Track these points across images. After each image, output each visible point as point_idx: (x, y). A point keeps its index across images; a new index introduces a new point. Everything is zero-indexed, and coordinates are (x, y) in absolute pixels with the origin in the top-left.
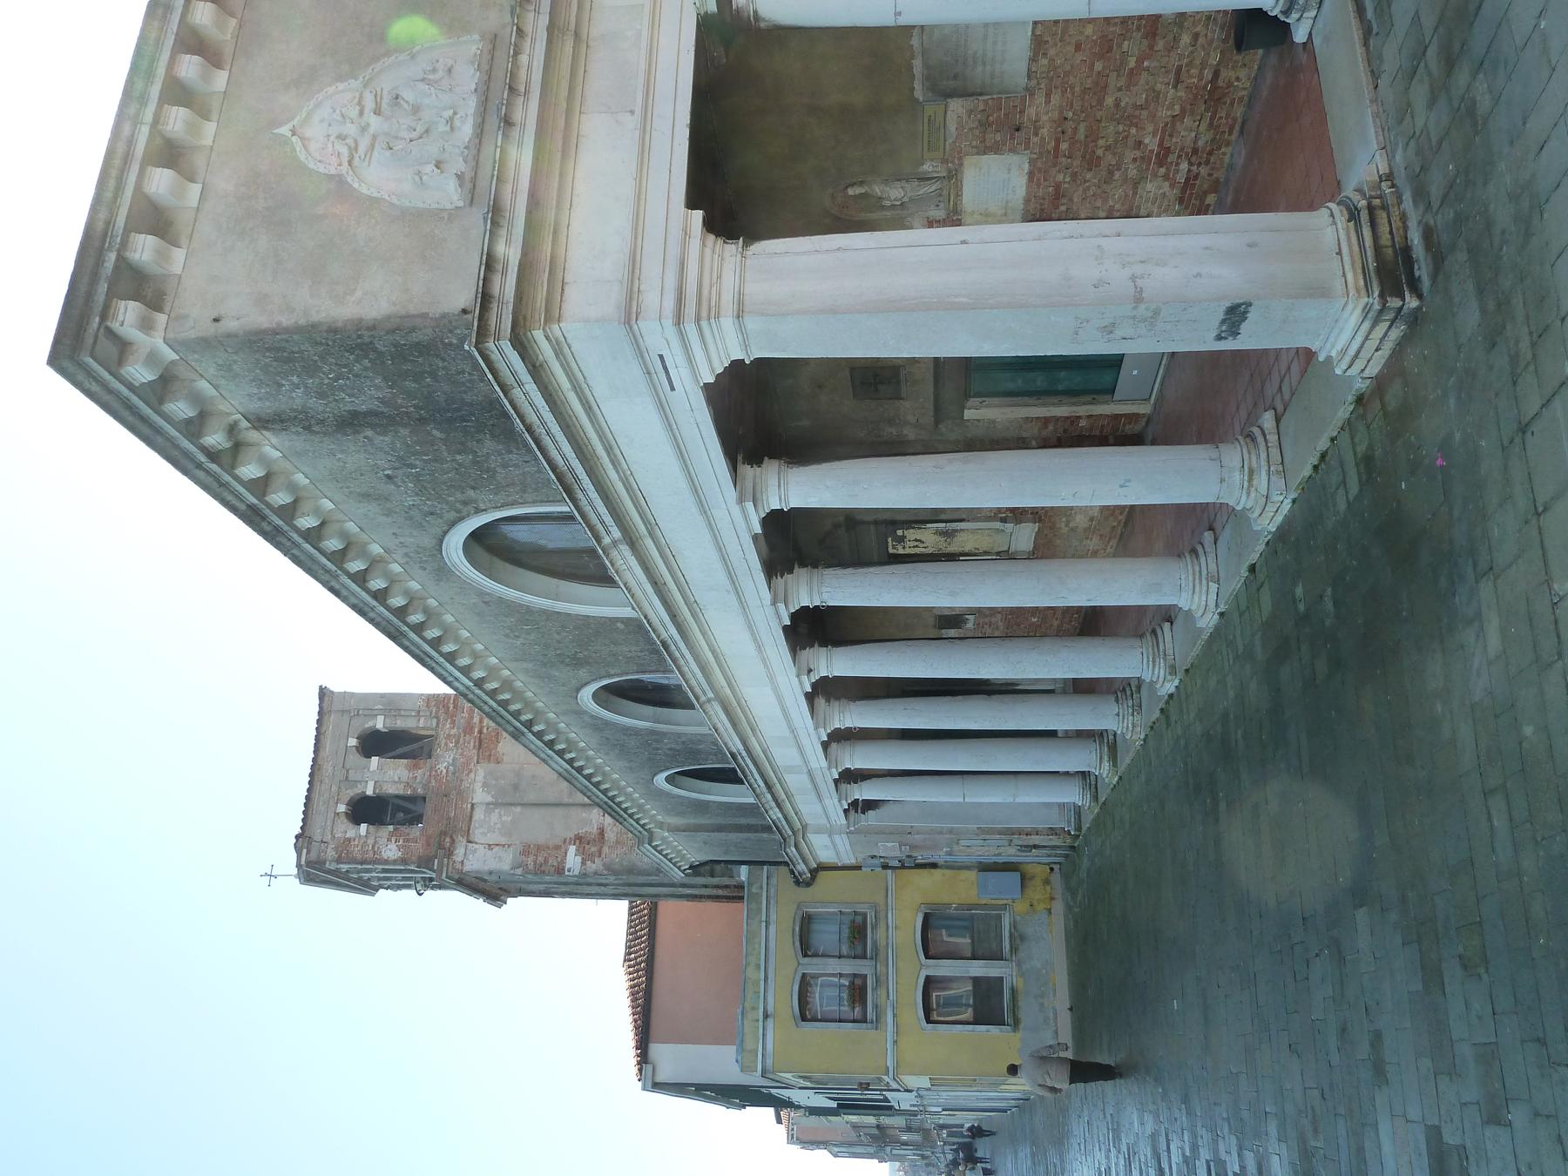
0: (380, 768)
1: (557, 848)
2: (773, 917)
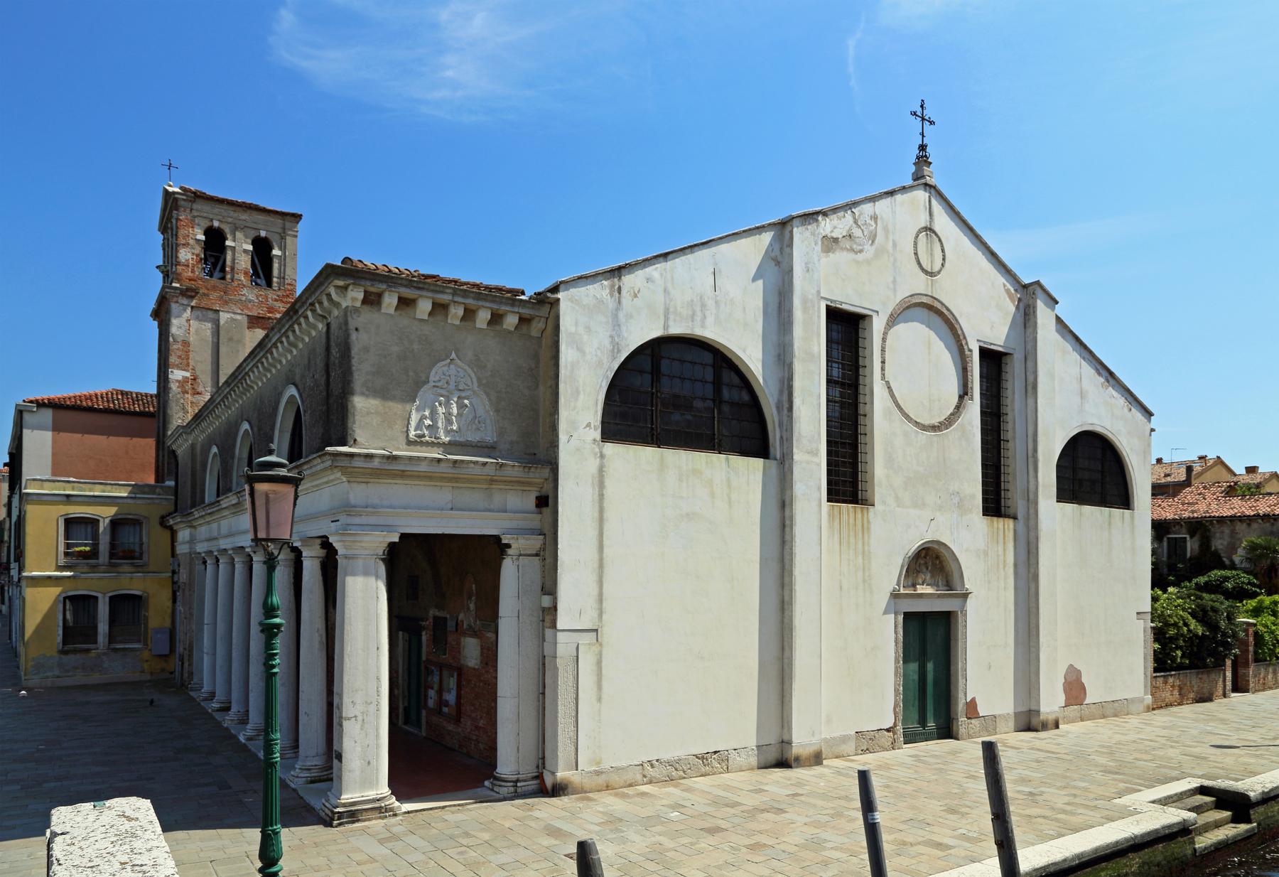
0: (245, 251)
1: (188, 365)
2: (139, 502)
